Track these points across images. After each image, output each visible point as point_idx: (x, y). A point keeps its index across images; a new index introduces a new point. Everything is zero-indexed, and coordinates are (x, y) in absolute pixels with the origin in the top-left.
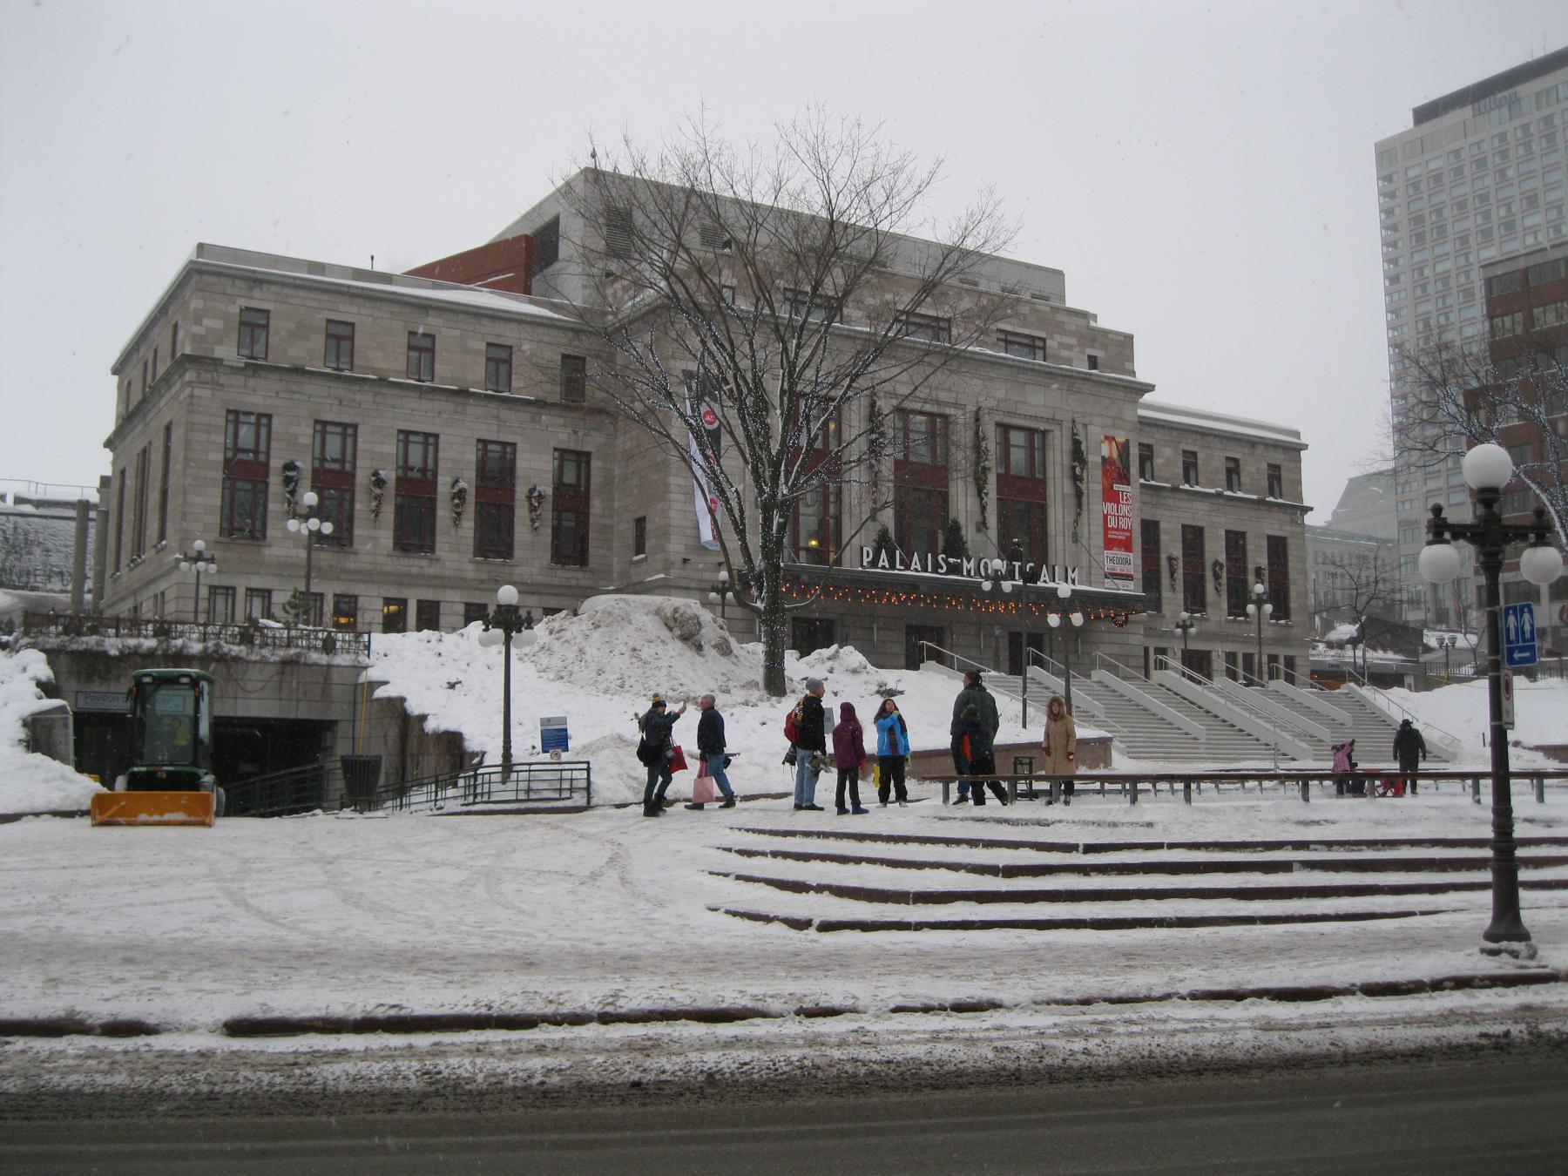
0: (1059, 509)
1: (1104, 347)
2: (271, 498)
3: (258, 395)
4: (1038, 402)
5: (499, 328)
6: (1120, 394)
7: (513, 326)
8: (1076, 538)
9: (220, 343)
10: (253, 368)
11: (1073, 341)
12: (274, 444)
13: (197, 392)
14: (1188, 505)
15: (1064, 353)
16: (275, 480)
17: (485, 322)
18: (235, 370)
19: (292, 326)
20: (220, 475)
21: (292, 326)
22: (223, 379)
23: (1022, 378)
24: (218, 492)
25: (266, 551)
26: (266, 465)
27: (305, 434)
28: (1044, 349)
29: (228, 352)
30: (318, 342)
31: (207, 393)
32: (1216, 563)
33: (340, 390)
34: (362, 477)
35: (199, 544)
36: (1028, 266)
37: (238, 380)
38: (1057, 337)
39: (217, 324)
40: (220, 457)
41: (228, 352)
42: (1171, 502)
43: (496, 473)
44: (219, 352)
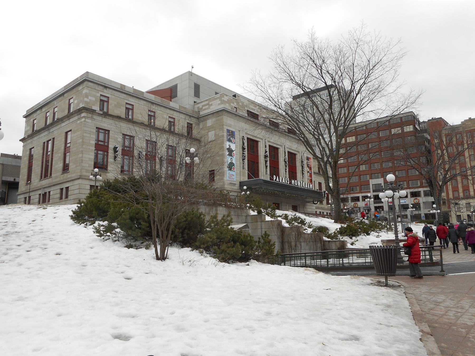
2: (109, 157)
3: (106, 123)
5: (172, 112)
9: (94, 105)
10: (106, 115)
12: (110, 140)
13: (87, 120)
16: (111, 152)
17: (168, 110)
18: (99, 115)
19: (116, 103)
21: (116, 103)
22: (95, 117)
25: (108, 174)
26: (108, 146)
27: (120, 139)
29: (96, 108)
30: (123, 110)
31: (90, 121)
33: (130, 126)
37: (100, 118)
39: (93, 99)
40: (94, 142)
41: (96, 108)
44: (94, 108)
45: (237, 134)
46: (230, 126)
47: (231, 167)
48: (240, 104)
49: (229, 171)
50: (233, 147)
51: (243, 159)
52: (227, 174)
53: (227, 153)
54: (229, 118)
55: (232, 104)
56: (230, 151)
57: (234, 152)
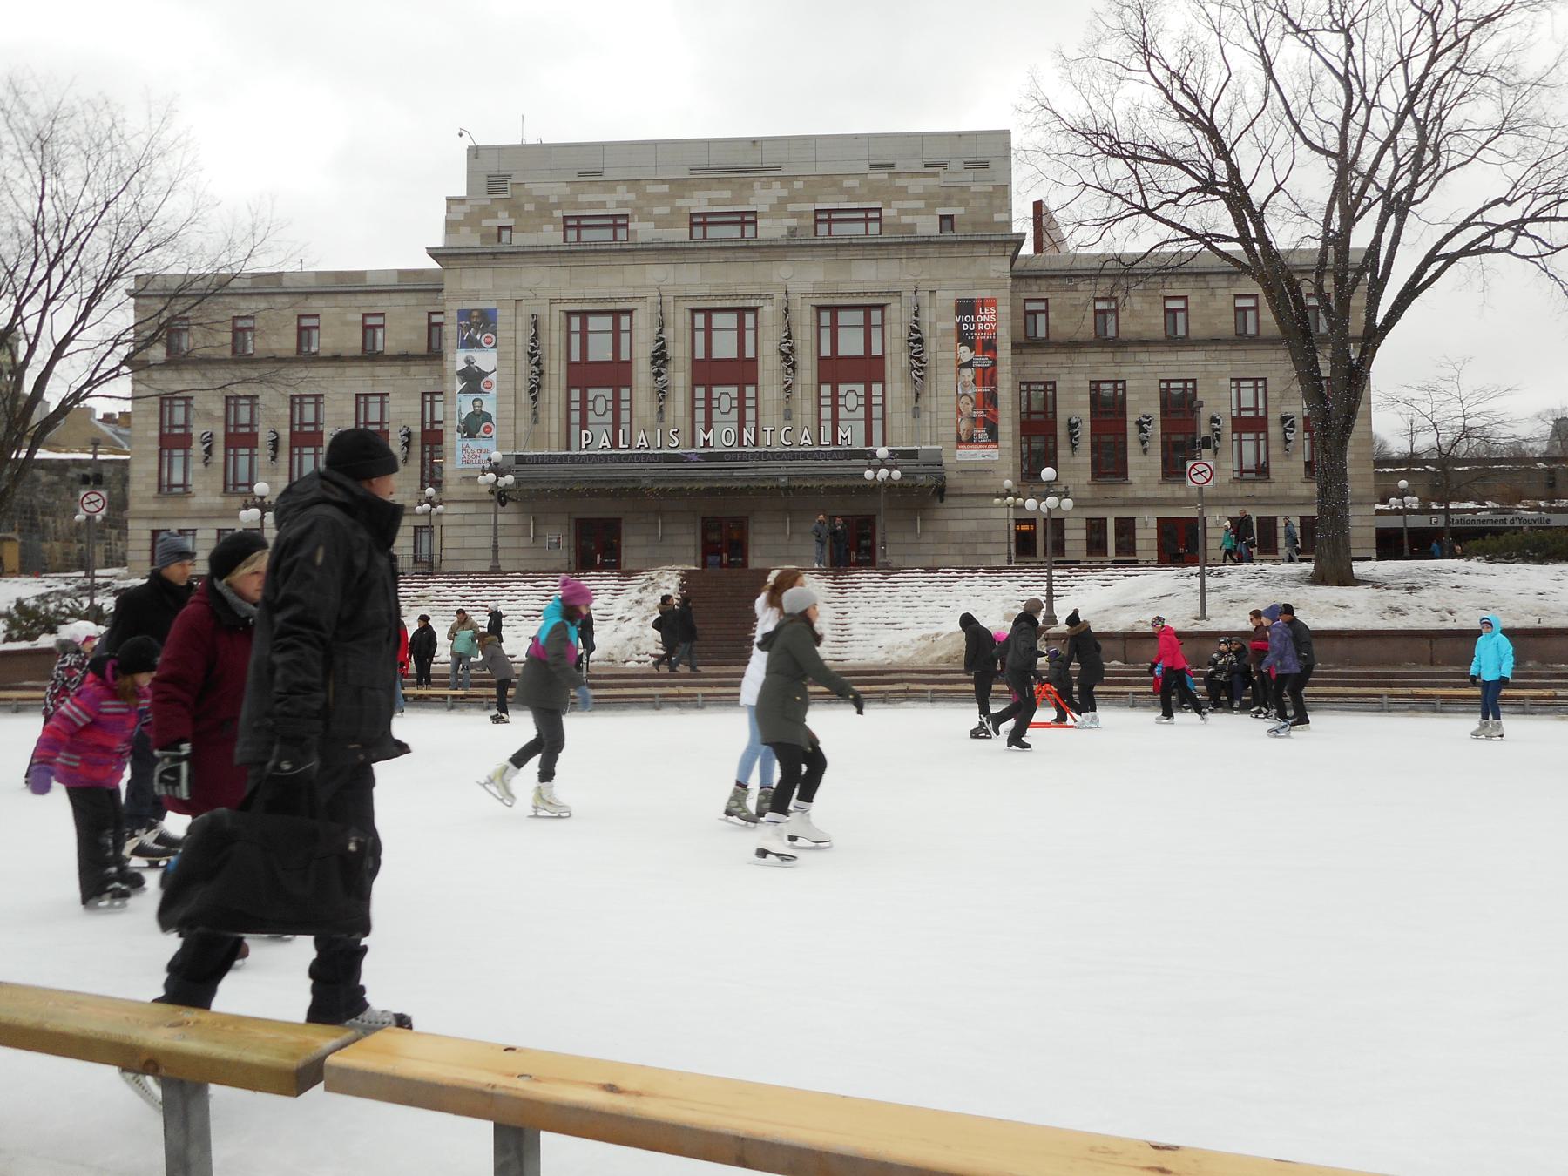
0: (898, 385)
1: (963, 203)
4: (866, 276)
5: (372, 299)
6: (984, 250)
7: (384, 296)
8: (916, 413)
11: (921, 204)
14: (1172, 357)
15: (906, 219)
17: (361, 297)
20: (156, 447)
23: (844, 254)
24: (156, 459)
25: (192, 501)
28: (879, 219)
32: (1214, 420)
34: (264, 436)
35: (1008, 483)
36: (960, 135)
38: (897, 204)
42: (1143, 357)
43: (1108, 410)
45: (504, 318)
46: (475, 295)
47: (473, 426)
48: (529, 207)
49: (469, 442)
50: (485, 360)
51: (535, 390)
52: (459, 453)
53: (459, 387)
54: (470, 273)
55: (485, 223)
56: (473, 379)
57: (493, 377)
